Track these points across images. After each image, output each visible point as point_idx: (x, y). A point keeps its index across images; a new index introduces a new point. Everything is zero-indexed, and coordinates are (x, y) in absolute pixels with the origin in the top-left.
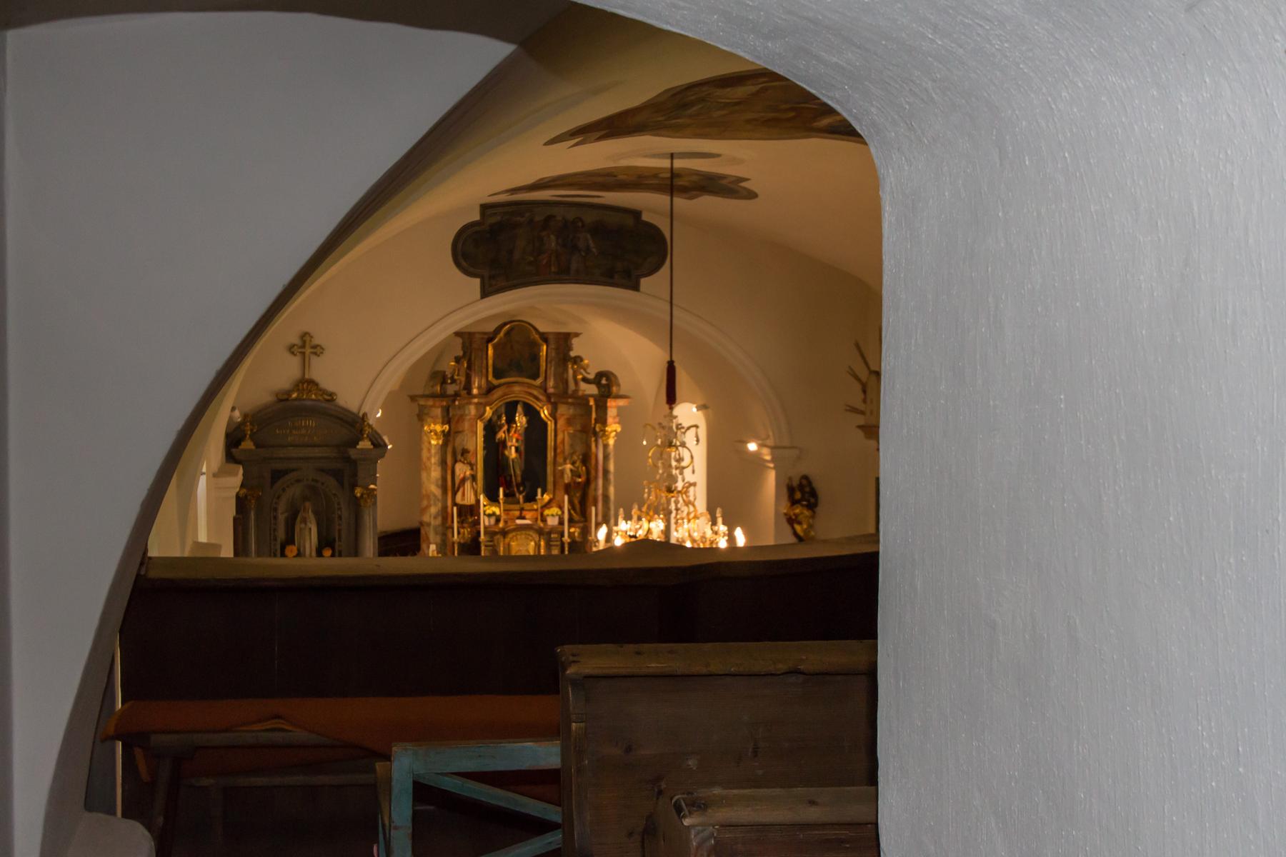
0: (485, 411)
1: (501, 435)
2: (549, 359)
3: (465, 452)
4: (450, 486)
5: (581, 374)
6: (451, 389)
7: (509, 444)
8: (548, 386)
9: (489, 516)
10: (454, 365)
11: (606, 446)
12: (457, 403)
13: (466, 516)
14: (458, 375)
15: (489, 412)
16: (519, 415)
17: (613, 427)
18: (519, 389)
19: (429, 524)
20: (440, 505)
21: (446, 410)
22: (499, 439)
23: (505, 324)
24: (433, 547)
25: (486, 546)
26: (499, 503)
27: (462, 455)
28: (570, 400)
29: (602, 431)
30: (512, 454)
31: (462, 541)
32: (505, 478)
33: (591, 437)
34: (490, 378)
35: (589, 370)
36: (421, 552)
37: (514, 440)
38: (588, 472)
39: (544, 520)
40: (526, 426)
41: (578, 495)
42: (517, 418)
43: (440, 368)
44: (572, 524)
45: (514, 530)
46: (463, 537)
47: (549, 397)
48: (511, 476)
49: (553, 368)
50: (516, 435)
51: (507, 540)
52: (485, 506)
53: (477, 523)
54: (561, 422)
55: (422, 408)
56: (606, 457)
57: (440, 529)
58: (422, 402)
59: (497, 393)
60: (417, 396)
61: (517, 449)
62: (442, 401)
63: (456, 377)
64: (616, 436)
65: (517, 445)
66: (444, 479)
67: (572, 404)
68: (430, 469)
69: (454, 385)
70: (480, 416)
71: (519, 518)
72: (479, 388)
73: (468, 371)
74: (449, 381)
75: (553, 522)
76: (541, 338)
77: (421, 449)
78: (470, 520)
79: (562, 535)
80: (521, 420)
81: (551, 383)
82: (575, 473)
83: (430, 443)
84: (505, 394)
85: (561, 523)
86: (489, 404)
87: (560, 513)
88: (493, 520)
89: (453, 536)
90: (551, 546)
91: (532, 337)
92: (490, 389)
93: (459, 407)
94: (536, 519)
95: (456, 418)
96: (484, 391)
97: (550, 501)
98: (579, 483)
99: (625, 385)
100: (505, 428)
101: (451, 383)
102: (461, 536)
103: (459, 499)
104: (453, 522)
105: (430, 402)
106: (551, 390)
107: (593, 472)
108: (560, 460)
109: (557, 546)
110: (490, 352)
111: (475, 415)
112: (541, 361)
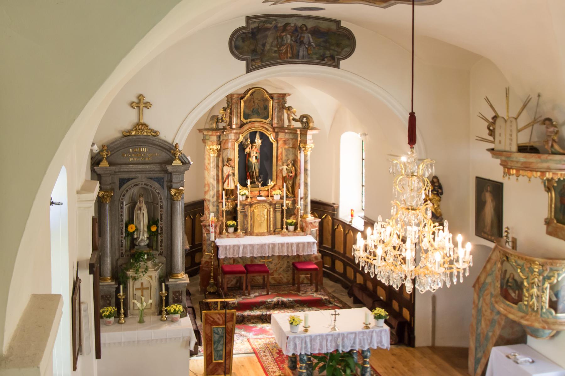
0: (239, 137)
1: (247, 150)
2: (274, 108)
3: (229, 160)
4: (221, 179)
6: (221, 125)
7: (252, 155)
8: (273, 123)
9: (242, 195)
11: (306, 156)
12: (225, 133)
13: (229, 196)
14: (225, 118)
15: (241, 138)
16: (257, 139)
17: (310, 144)
18: (257, 125)
19: (209, 201)
20: (215, 190)
21: (219, 137)
22: (246, 152)
23: (250, 89)
24: (212, 215)
25: (241, 212)
26: (247, 187)
27: (227, 162)
28: (286, 131)
29: (304, 147)
30: (253, 160)
32: (250, 173)
33: (298, 151)
34: (242, 119)
35: (296, 115)
36: (204, 215)
37: (255, 153)
38: (296, 170)
39: (272, 196)
40: (261, 144)
41: (291, 183)
42: (256, 141)
43: (216, 113)
44: (287, 199)
45: (256, 203)
46: (228, 207)
47: (274, 129)
48: (253, 172)
49: (276, 113)
50: (256, 150)
51: (252, 209)
52: (240, 189)
53: (236, 199)
54: (280, 143)
55: (204, 136)
56: (306, 162)
57: (216, 203)
58: (205, 133)
59: (246, 127)
60: (202, 129)
61: (256, 157)
62: (217, 132)
63: (224, 119)
64: (311, 150)
65: (256, 155)
66: (218, 175)
68: (210, 170)
69: (223, 123)
70: (237, 140)
71: (259, 196)
72: (236, 124)
73: (231, 115)
74: (220, 121)
76: (269, 97)
77: (205, 159)
78: (232, 198)
79: (282, 206)
80: (258, 141)
81: (275, 121)
82: (289, 171)
83: (209, 155)
84: (250, 128)
85: (282, 198)
87: (281, 193)
88: (244, 197)
89: (223, 207)
90: (276, 211)
91: (265, 96)
92: (242, 125)
93: (225, 135)
94: (268, 196)
95: (224, 141)
96: (239, 126)
98: (291, 176)
100: (250, 146)
101: (221, 122)
102: (227, 206)
104: (222, 199)
105: (210, 133)
106: (275, 125)
107: (298, 170)
108: (280, 163)
109: (279, 211)
111: (234, 140)
112: (270, 110)
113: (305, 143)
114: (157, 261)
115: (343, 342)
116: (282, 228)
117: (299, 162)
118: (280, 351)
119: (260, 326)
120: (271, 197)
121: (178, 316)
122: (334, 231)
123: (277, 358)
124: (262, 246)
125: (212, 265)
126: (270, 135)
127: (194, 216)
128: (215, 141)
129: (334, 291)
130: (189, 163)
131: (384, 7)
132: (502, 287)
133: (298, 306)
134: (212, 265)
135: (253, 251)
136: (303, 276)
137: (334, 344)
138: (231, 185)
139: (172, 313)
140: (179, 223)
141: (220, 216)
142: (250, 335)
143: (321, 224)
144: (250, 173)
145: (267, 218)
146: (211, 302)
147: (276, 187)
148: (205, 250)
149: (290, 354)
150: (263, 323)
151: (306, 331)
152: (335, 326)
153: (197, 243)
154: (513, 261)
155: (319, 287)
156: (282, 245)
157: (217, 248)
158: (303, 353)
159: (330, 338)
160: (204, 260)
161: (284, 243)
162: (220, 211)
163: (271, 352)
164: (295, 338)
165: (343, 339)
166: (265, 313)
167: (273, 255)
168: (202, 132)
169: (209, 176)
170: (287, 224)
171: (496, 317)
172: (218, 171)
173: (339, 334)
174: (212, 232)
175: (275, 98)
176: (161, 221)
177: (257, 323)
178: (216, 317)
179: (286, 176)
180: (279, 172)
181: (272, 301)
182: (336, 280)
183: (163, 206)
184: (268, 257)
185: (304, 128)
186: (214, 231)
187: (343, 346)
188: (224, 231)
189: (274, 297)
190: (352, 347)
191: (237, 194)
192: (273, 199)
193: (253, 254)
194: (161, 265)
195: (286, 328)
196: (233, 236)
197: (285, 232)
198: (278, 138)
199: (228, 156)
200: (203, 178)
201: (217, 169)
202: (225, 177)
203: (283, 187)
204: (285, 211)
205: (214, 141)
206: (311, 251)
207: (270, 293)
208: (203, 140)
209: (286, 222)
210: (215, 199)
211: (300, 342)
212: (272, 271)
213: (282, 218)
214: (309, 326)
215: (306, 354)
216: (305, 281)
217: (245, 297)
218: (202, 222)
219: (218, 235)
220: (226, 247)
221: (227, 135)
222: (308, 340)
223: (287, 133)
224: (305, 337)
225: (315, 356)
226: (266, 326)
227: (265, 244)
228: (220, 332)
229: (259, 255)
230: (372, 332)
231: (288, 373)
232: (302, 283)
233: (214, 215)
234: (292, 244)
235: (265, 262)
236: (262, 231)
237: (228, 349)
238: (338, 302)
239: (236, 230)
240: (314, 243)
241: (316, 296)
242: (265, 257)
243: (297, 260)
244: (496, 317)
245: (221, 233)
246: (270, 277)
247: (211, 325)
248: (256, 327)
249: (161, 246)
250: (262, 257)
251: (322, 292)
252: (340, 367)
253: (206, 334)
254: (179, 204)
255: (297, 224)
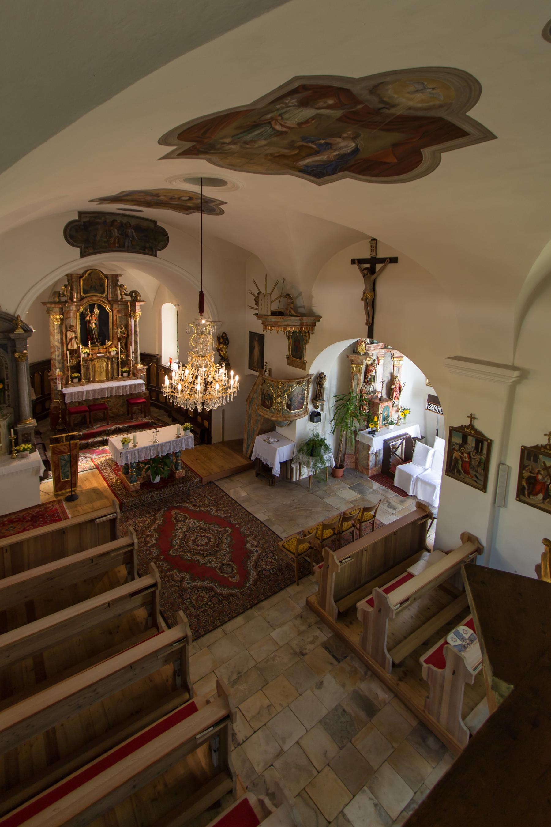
0: (80, 308)
1: (88, 318)
2: (109, 286)
3: (71, 326)
4: (65, 342)
5: (124, 292)
6: (63, 299)
7: (92, 322)
9: (84, 353)
10: (64, 289)
11: (135, 321)
12: (66, 305)
14: (66, 293)
15: (82, 309)
17: (138, 313)
19: (55, 359)
20: (60, 350)
21: (62, 308)
22: (87, 320)
23: (88, 270)
24: (58, 370)
25: (83, 366)
26: (88, 347)
27: (70, 328)
28: (119, 303)
29: (134, 315)
31: (72, 365)
32: (90, 336)
34: (82, 294)
35: (127, 290)
36: (52, 371)
37: (94, 320)
38: (128, 332)
39: (109, 353)
41: (124, 342)
42: (95, 311)
45: (96, 358)
46: (73, 363)
47: (109, 301)
49: (110, 290)
50: (95, 318)
51: (93, 363)
54: (115, 312)
55: (48, 308)
56: (135, 326)
57: (61, 361)
58: (49, 305)
59: (86, 300)
61: (95, 324)
64: (139, 317)
65: (95, 322)
66: (62, 339)
67: (120, 304)
68: (54, 335)
72: (77, 298)
73: (71, 291)
75: (113, 353)
79: (118, 359)
80: (97, 311)
81: (110, 296)
83: (54, 324)
84: (89, 301)
85: (117, 353)
86: (82, 305)
87: (116, 349)
88: (86, 355)
89: (68, 363)
90: (113, 363)
93: (67, 307)
94: (106, 353)
95: (66, 312)
97: (111, 344)
99: (142, 296)
100: (90, 315)
102: (71, 363)
103: (69, 347)
104: (67, 357)
105: (53, 305)
108: (115, 327)
109: (115, 363)
110: (81, 282)
113: (135, 312)
114: (5, 412)
115: (162, 449)
116: (118, 375)
117: (130, 326)
118: (117, 463)
119: (101, 448)
120: (108, 353)
121: (28, 452)
122: (158, 373)
123: (115, 468)
124: (102, 390)
125: (60, 409)
126: (106, 306)
127: (43, 373)
128: (58, 311)
129: (159, 416)
130: (32, 331)
131: (187, 214)
132: (262, 400)
133: (131, 430)
134: (60, 409)
135: (95, 395)
136: (135, 408)
137: (155, 452)
138: (74, 346)
139: (22, 451)
140: (24, 380)
141: (65, 371)
142: (94, 456)
143: (148, 370)
144: (90, 336)
145: (106, 369)
146: (60, 437)
147: (113, 346)
148: (53, 398)
149: (123, 464)
150: (104, 445)
151: (135, 446)
152: (156, 439)
153: (46, 393)
154: (268, 383)
155: (147, 414)
156: (118, 387)
157: (64, 395)
158: (133, 462)
159: (152, 448)
160: (53, 406)
161: (120, 386)
162: (66, 367)
163: (110, 465)
164: (126, 453)
165: (162, 447)
166: (105, 438)
167: (111, 396)
168: (46, 305)
169: (54, 340)
170: (122, 372)
171: (259, 418)
172: (62, 335)
173: (159, 445)
174: (59, 384)
175: (110, 278)
176: (7, 379)
177: (99, 446)
178: (62, 448)
179: (120, 337)
180: (114, 334)
181: (111, 429)
182: (159, 407)
183: (8, 368)
184: (108, 398)
185: (134, 301)
186: (60, 382)
187: (162, 452)
188: (70, 382)
189: (112, 426)
190: (168, 451)
191: (80, 352)
192: (110, 355)
193: (95, 397)
194: (9, 415)
195: (120, 446)
196: (78, 384)
197: (120, 378)
198: (113, 309)
199: (70, 323)
200: (49, 341)
201: (60, 334)
202: (68, 340)
203: (118, 345)
204: (120, 363)
205: (57, 312)
206: (141, 390)
207: (109, 423)
208: (47, 311)
209: (121, 370)
210: (60, 357)
211: (131, 455)
212: (111, 408)
213: (118, 368)
214: (137, 443)
215: (135, 462)
216: (137, 411)
217: (89, 429)
218: (49, 376)
219: (64, 385)
220: (71, 394)
221: (69, 307)
222: (136, 452)
223: (120, 304)
224: (134, 450)
225: (142, 462)
226: (107, 448)
227: (104, 389)
228: (66, 459)
229: (100, 397)
230: (182, 439)
231: (123, 477)
232: (135, 413)
233: (60, 370)
234: (126, 386)
235: (105, 401)
236: (102, 379)
237: (73, 470)
238: (161, 422)
239: (80, 380)
240: (143, 384)
241: (145, 420)
242: (104, 398)
243: (130, 397)
244: (259, 418)
245: (67, 383)
246: (109, 412)
247: (58, 454)
248: (98, 449)
249: (9, 400)
250: (102, 398)
251: (150, 418)
252: (160, 466)
253: (54, 462)
254: (23, 364)
255: (130, 372)
